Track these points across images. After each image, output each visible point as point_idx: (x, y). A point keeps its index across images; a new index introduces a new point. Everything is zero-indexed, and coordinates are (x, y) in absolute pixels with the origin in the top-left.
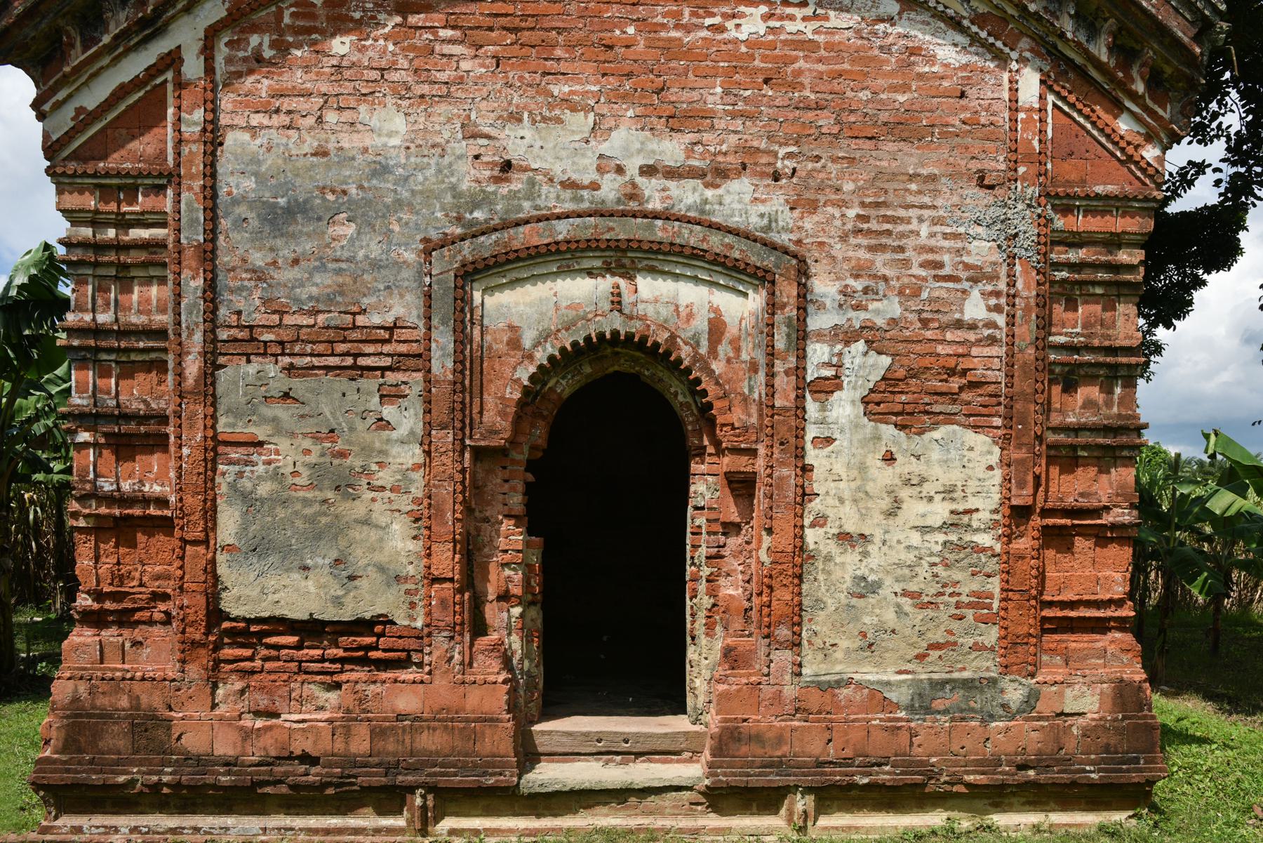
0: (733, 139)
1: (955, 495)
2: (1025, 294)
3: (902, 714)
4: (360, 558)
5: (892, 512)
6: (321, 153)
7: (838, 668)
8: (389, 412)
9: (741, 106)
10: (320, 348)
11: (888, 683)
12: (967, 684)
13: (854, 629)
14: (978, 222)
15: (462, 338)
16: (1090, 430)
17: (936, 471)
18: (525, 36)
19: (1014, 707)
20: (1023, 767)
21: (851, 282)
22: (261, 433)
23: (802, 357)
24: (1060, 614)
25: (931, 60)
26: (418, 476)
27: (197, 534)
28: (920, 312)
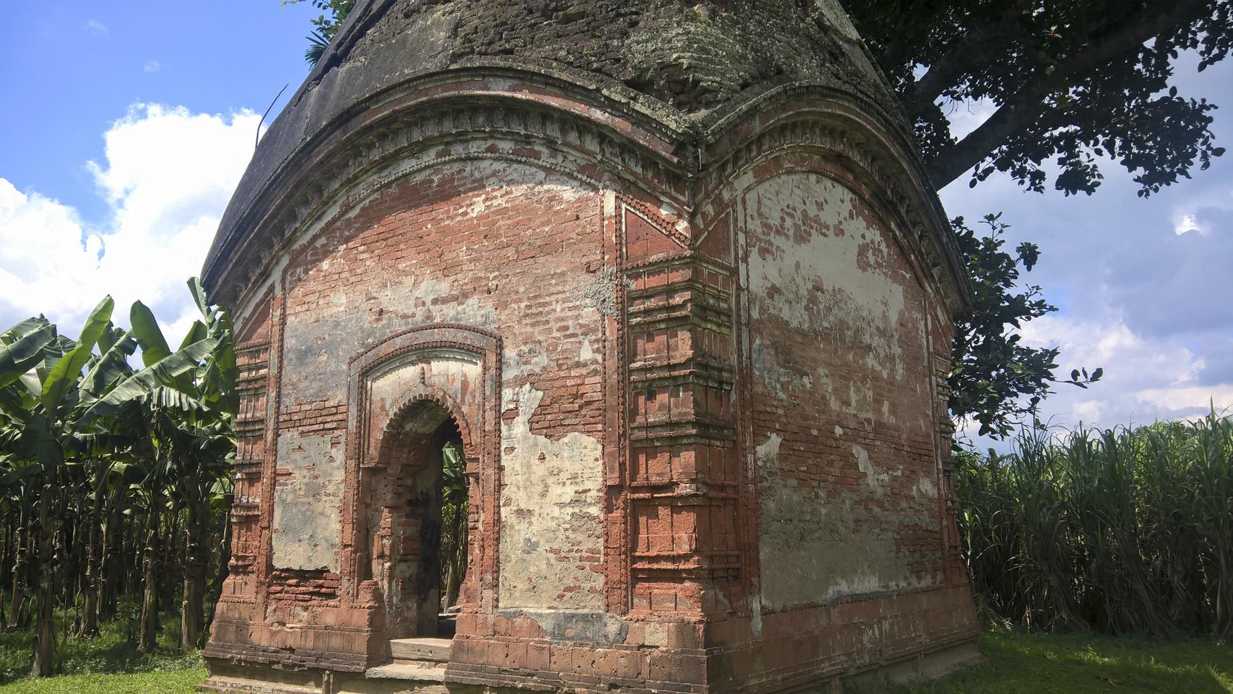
3: (548, 639)
4: (320, 534)
5: (543, 495)
7: (517, 603)
8: (334, 452)
10: (312, 421)
11: (540, 615)
12: (585, 618)
13: (524, 575)
17: (567, 464)
19: (611, 637)
21: (523, 348)
23: (499, 398)
24: (647, 566)
25: (561, 201)
27: (265, 524)
28: (557, 360)
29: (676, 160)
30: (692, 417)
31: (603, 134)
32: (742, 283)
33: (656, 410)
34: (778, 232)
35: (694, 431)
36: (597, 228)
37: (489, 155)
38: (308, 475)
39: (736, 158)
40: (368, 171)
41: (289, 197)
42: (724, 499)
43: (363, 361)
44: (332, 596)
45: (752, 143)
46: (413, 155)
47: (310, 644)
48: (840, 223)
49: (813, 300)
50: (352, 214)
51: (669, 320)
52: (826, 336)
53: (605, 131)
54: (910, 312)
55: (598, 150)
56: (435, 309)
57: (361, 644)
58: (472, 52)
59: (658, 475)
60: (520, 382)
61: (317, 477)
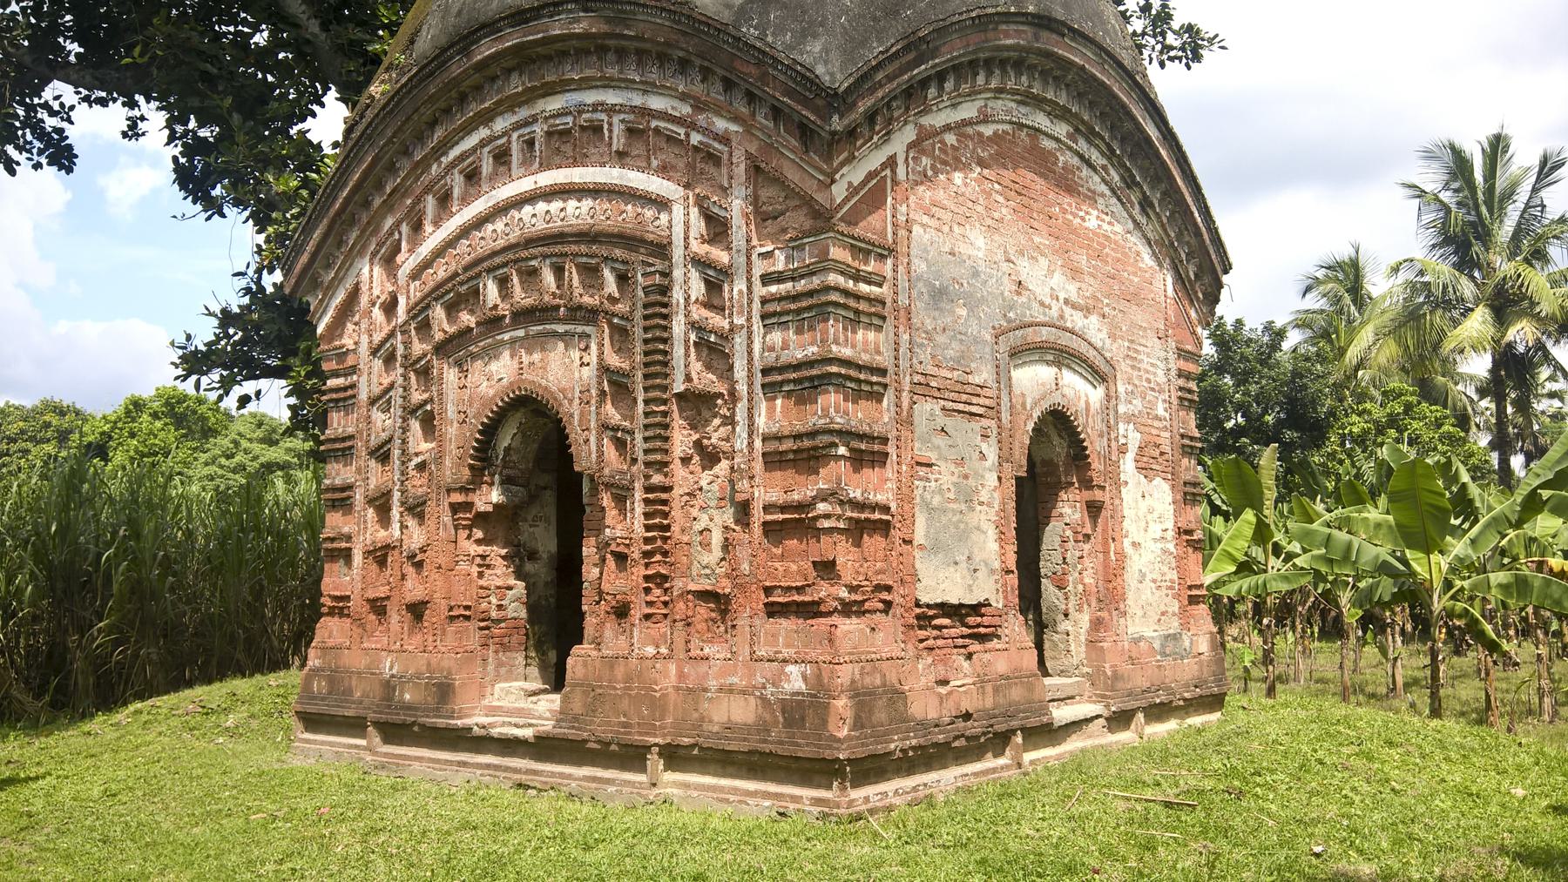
8: (984, 447)
22: (932, 456)
47: (989, 702)
61: (966, 477)
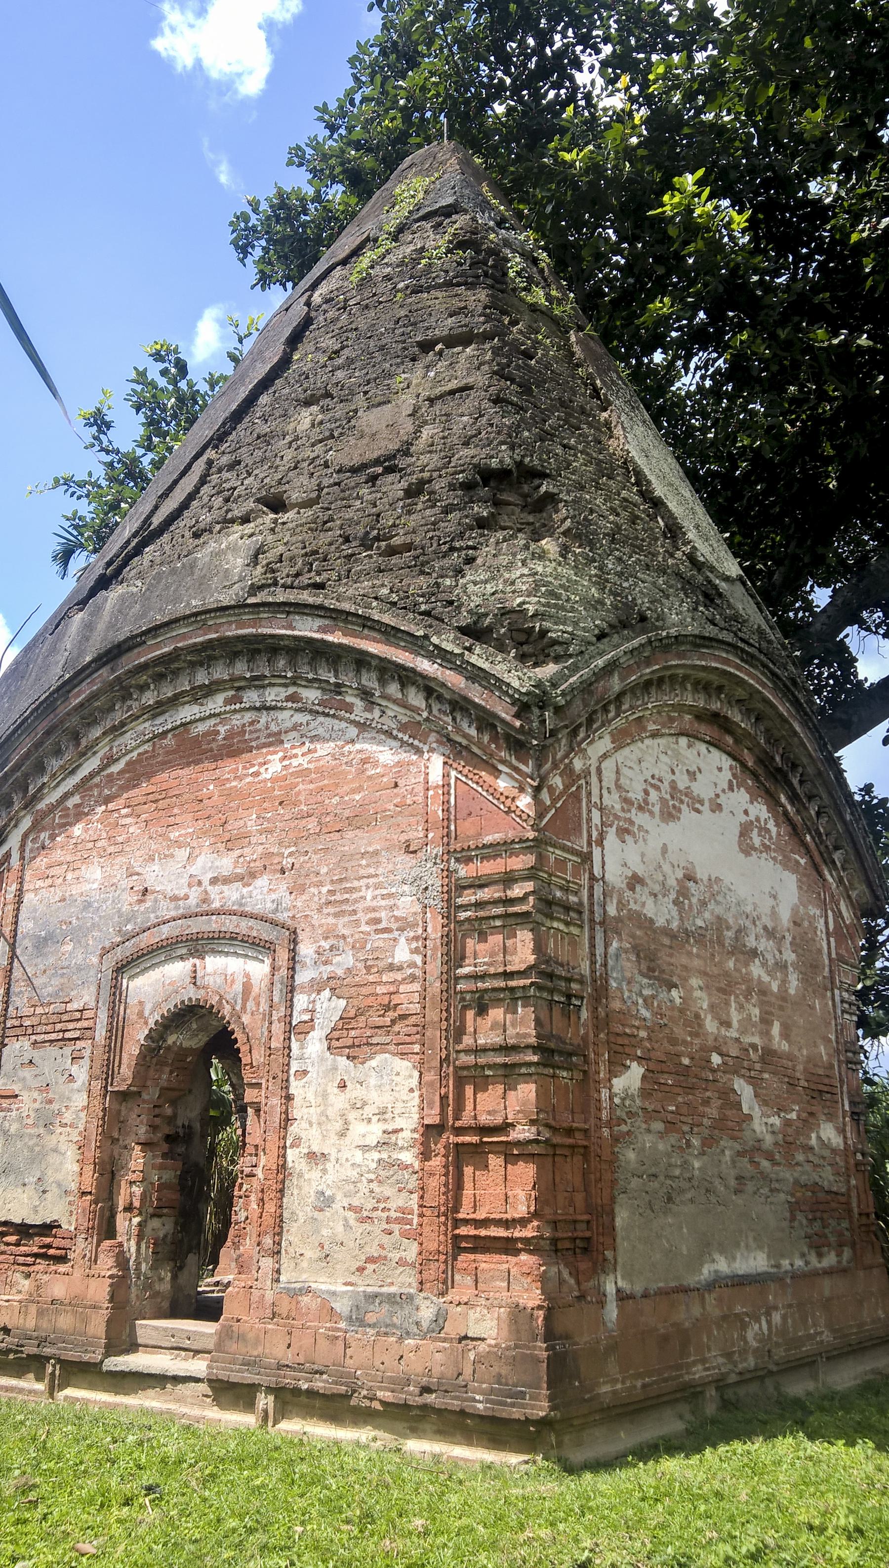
0: (260, 849)
1: (387, 1116)
2: (433, 936)
3: (342, 1325)
5: (342, 1135)
6: (63, 900)
7: (304, 1277)
8: (74, 1070)
9: (266, 825)
10: (49, 1028)
11: (334, 1293)
12: (391, 1299)
13: (315, 1240)
14: (403, 882)
15: (113, 1014)
16: (494, 1050)
18: (161, 804)
19: (425, 1325)
20: (426, 1390)
24: (473, 1232)
25: (376, 764)
26: (83, 1115)
29: (518, 723)
30: (533, 1041)
31: (430, 689)
32: (597, 871)
33: (489, 1029)
34: (640, 808)
35: (535, 1058)
36: (420, 799)
37: (290, 704)
38: (39, 1098)
39: (590, 721)
40: (138, 717)
41: (37, 745)
42: (572, 1147)
43: (120, 954)
44: (62, 1259)
45: (609, 702)
46: (196, 700)
47: (31, 1323)
48: (717, 796)
49: (683, 892)
50: (115, 769)
51: (507, 915)
52: (700, 937)
53: (432, 684)
54: (805, 907)
55: (423, 706)
56: (214, 891)
57: (97, 1326)
58: (275, 584)
59: (489, 1113)
60: (317, 986)
61: (50, 1102)
